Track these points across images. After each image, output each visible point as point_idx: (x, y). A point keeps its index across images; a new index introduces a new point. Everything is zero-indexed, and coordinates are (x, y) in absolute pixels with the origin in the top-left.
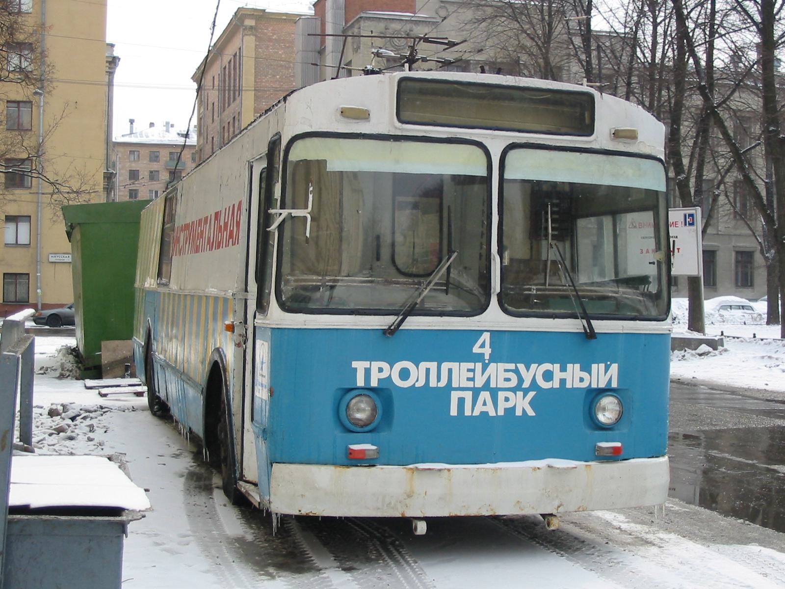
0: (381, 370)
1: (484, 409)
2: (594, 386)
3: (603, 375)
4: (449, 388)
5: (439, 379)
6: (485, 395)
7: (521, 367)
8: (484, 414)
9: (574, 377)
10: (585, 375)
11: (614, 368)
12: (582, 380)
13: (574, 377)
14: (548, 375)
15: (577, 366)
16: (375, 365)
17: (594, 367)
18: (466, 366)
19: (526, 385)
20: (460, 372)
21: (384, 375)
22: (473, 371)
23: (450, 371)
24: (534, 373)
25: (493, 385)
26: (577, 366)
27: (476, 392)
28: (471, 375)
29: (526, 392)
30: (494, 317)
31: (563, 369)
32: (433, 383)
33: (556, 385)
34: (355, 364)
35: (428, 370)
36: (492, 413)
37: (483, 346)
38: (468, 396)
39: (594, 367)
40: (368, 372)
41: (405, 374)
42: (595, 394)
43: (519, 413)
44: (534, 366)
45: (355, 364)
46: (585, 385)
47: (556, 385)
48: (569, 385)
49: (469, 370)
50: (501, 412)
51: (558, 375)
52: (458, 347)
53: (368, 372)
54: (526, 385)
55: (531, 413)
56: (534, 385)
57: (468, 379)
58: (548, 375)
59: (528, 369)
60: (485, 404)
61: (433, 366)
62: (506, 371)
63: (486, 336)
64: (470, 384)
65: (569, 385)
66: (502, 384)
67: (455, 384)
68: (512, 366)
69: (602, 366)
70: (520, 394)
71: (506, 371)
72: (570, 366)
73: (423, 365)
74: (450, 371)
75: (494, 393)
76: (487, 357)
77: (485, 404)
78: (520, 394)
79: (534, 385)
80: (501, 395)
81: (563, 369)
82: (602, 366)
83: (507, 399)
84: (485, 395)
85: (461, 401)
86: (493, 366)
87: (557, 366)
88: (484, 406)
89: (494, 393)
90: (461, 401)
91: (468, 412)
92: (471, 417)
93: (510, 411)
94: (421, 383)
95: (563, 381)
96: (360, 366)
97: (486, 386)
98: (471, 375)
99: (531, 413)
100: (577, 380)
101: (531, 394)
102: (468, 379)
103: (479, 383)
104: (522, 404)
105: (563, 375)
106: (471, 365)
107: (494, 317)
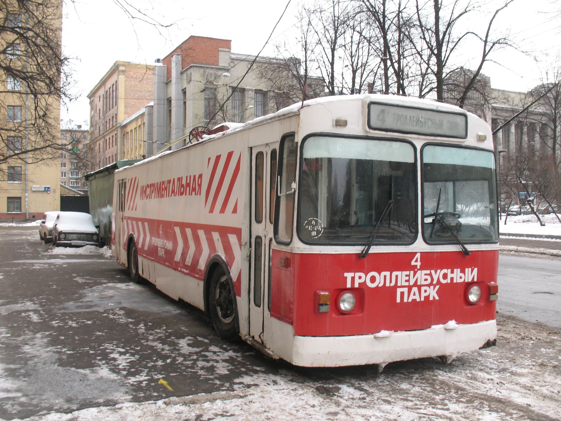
0: (360, 278)
1: (414, 297)
2: (466, 281)
3: (471, 275)
5: (391, 282)
6: (415, 289)
7: (433, 272)
8: (414, 300)
9: (458, 276)
10: (462, 275)
11: (476, 270)
12: (461, 278)
13: (458, 276)
14: (445, 276)
15: (459, 270)
16: (358, 274)
19: (435, 282)
20: (402, 276)
21: (362, 281)
22: (409, 276)
23: (397, 276)
24: (438, 275)
25: (419, 283)
27: (410, 288)
28: (407, 278)
30: (420, 246)
31: (452, 272)
32: (388, 285)
33: (449, 282)
34: (346, 274)
35: (385, 276)
36: (418, 300)
37: (416, 261)
38: (406, 290)
39: (467, 270)
40: (353, 279)
41: (373, 279)
42: (467, 286)
43: (431, 299)
44: (439, 271)
45: (346, 274)
48: (455, 281)
49: (406, 276)
50: (423, 299)
51: (450, 275)
52: (402, 262)
53: (353, 279)
54: (435, 282)
56: (439, 282)
57: (406, 281)
58: (445, 276)
59: (436, 273)
60: (414, 294)
61: (387, 274)
62: (425, 275)
63: (418, 255)
64: (407, 284)
65: (455, 281)
67: (399, 284)
68: (428, 272)
69: (470, 269)
70: (432, 287)
71: (425, 275)
72: (455, 270)
73: (383, 273)
74: (397, 276)
75: (419, 288)
76: (418, 267)
77: (414, 294)
79: (439, 282)
80: (423, 289)
81: (452, 272)
82: (470, 269)
83: (426, 291)
84: (415, 289)
85: (402, 294)
87: (450, 270)
88: (415, 296)
89: (419, 288)
90: (402, 294)
91: (405, 300)
92: (408, 302)
93: (427, 298)
94: (380, 285)
95: (452, 279)
96: (349, 275)
97: (415, 284)
98: (407, 278)
99: (437, 298)
100: (459, 277)
101: (437, 287)
102: (406, 281)
103: (412, 283)
104: (433, 293)
105: (452, 275)
106: (407, 273)
107: (420, 246)
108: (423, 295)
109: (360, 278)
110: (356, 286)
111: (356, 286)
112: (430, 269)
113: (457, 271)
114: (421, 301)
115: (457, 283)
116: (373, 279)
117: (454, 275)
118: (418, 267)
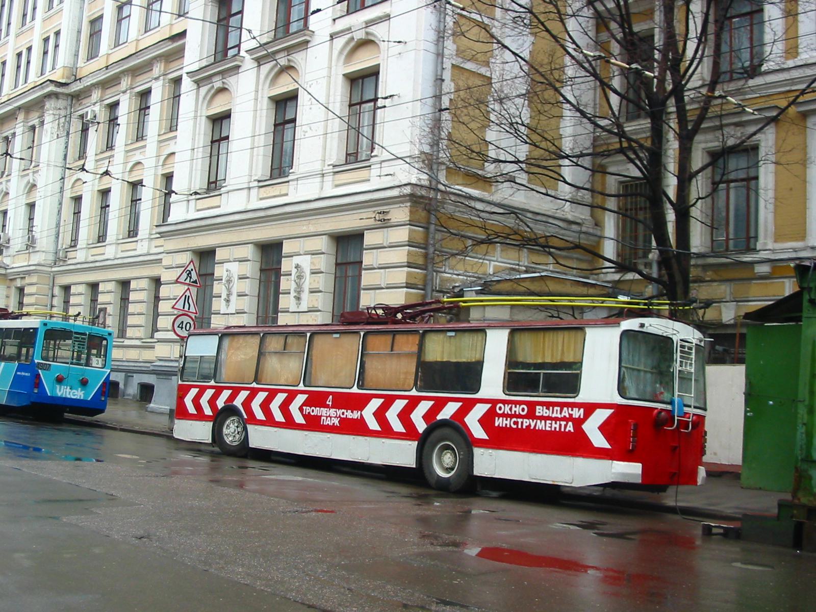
6: (329, 418)
14: (343, 413)
18: (326, 409)
20: (323, 411)
24: (340, 412)
38: (325, 418)
41: (313, 411)
46: (351, 417)
47: (345, 416)
51: (346, 413)
54: (338, 416)
55: (338, 425)
58: (343, 413)
61: (318, 409)
66: (333, 415)
68: (335, 410)
75: (331, 417)
79: (340, 417)
80: (332, 419)
84: (329, 418)
93: (334, 424)
97: (329, 416)
99: (338, 425)
101: (339, 419)
103: (328, 415)
108: (332, 422)
113: (349, 411)
115: (349, 419)
116: (313, 411)
117: (347, 414)
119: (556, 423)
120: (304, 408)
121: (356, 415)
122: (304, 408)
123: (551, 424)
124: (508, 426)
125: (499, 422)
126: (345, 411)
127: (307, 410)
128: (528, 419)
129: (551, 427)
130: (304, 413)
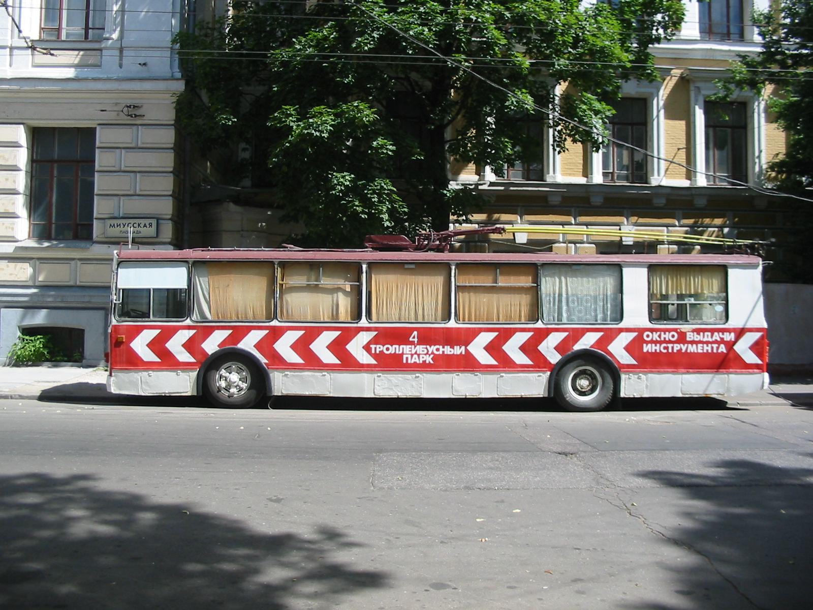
0: (380, 348)
4: (403, 354)
5: (399, 351)
7: (428, 347)
14: (438, 350)
16: (378, 346)
17: (455, 347)
19: (430, 352)
20: (406, 349)
23: (403, 348)
24: (432, 349)
25: (418, 352)
26: (449, 347)
27: (412, 355)
29: (430, 355)
31: (443, 347)
32: (397, 352)
34: (371, 346)
35: (395, 348)
37: (414, 337)
38: (409, 356)
39: (455, 347)
40: (375, 348)
41: (388, 349)
45: (371, 346)
46: (452, 353)
47: (441, 352)
48: (446, 353)
53: (375, 348)
54: (430, 352)
56: (433, 353)
58: (438, 350)
63: (415, 333)
64: (410, 353)
65: (446, 353)
66: (421, 352)
67: (405, 352)
68: (425, 346)
69: (458, 347)
70: (428, 356)
72: (446, 347)
73: (394, 346)
74: (403, 348)
75: (419, 355)
76: (416, 342)
78: (428, 356)
79: (433, 353)
80: (421, 356)
81: (443, 347)
82: (458, 347)
84: (416, 356)
86: (418, 347)
89: (419, 355)
92: (411, 364)
93: (424, 362)
94: (393, 352)
95: (443, 352)
97: (416, 353)
101: (432, 356)
103: (413, 352)
104: (429, 359)
106: (410, 346)
109: (380, 348)
110: (378, 352)
111: (378, 352)
112: (426, 345)
114: (420, 364)
115: (447, 355)
116: (388, 349)
118: (416, 342)
119: (707, 346)
120: (373, 346)
121: (458, 350)
122: (373, 346)
123: (703, 347)
124: (658, 351)
125: (647, 348)
126: (441, 347)
127: (379, 348)
128: (679, 343)
129: (703, 350)
130: (373, 352)
